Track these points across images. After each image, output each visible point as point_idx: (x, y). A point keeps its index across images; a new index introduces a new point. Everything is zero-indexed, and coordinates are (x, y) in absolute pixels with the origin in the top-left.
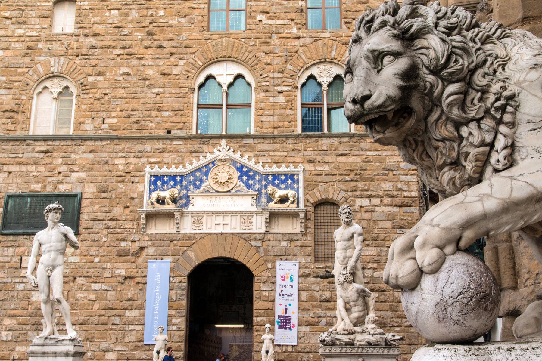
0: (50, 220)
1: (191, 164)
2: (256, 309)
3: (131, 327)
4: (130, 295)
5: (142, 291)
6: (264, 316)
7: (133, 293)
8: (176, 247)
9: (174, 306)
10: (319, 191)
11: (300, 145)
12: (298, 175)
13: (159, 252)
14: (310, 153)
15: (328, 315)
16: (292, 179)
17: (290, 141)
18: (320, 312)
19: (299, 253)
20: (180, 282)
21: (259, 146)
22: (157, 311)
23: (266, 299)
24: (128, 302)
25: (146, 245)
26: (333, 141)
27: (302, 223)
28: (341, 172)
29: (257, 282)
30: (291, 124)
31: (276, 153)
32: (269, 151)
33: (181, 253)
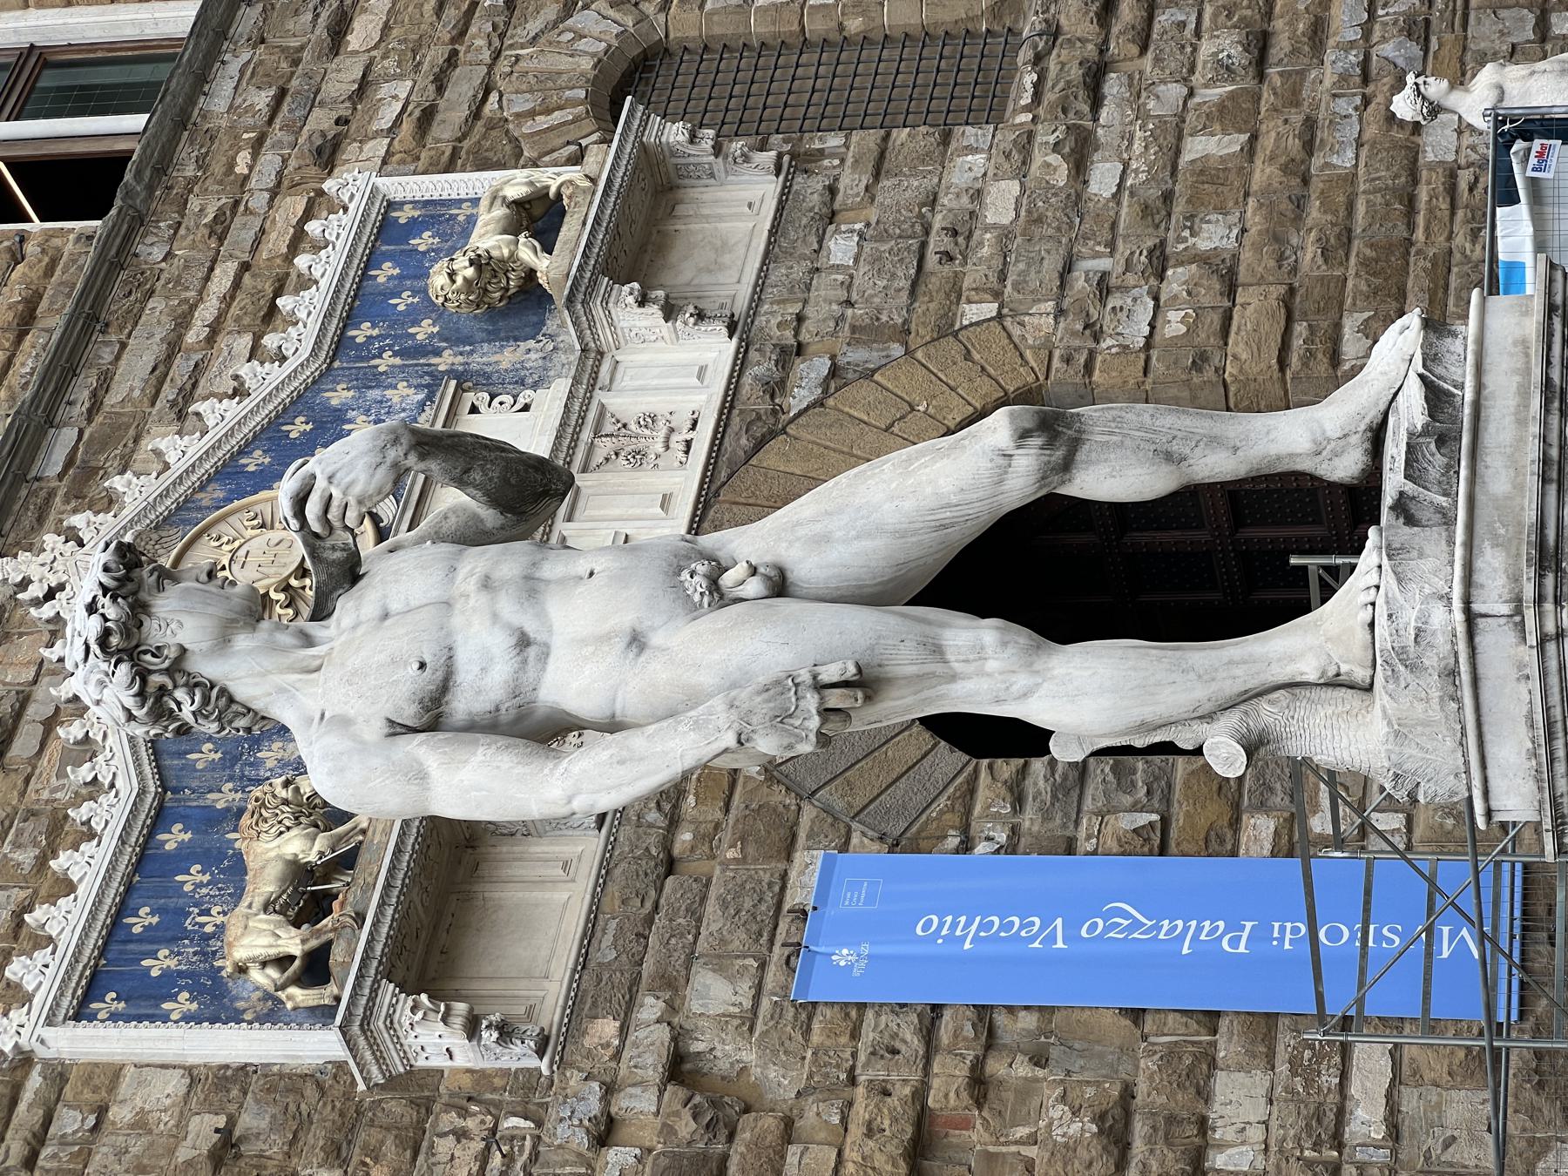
0: (223, 640)
1: (86, 748)
2: (1283, 364)
3: (1366, 1120)
4: (1081, 1128)
5: (1055, 1053)
6: (1338, 326)
7: (1058, 1111)
8: (726, 836)
9: (1202, 823)
10: (532, 114)
11: (194, 204)
12: (391, 205)
13: (738, 941)
14: (270, 161)
15: (1354, 34)
16: (414, 227)
17: (152, 251)
18: (1337, 61)
19: (916, 186)
20: (1018, 801)
21: (112, 399)
22: (1234, 927)
23: (1215, 319)
24: (1138, 1147)
25: (663, 1034)
26: (234, 67)
27: (717, 150)
28: (445, 33)
29: (1089, 368)
30: (31, 248)
31: (207, 312)
32: (174, 346)
33: (778, 796)
